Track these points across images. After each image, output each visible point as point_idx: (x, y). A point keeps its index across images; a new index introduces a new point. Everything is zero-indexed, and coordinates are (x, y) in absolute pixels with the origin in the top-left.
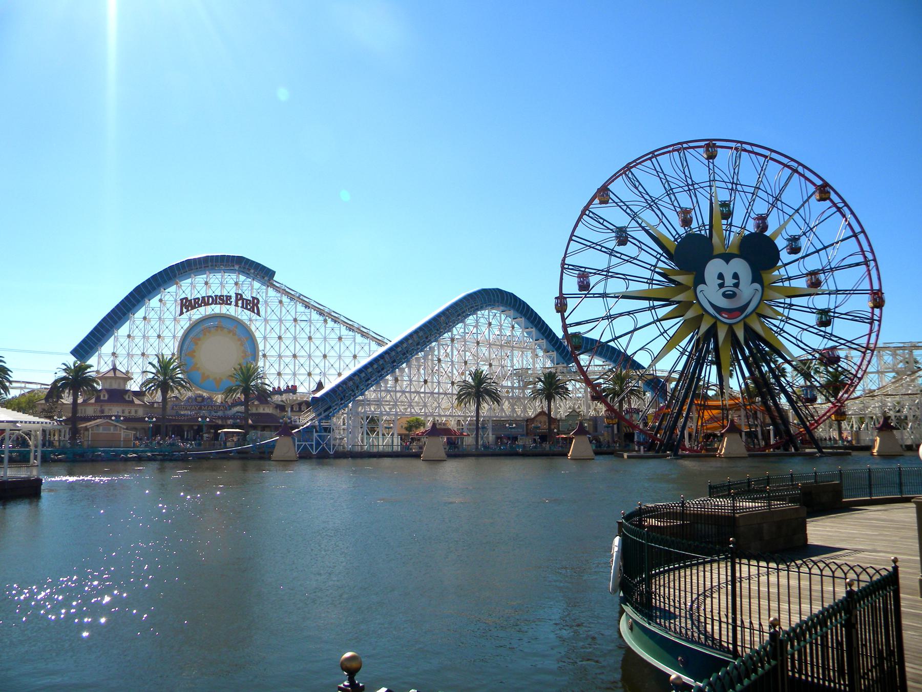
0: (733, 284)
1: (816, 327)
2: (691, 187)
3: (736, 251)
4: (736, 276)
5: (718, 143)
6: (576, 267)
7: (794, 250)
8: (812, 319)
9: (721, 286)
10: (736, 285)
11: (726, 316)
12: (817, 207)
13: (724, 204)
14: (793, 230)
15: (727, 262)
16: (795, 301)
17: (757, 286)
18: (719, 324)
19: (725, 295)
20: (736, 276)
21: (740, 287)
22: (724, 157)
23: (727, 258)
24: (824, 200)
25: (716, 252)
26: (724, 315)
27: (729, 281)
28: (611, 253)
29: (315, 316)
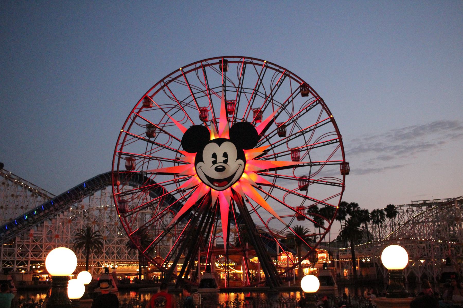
0: (223, 161)
1: (299, 192)
2: (209, 92)
3: (227, 137)
4: (225, 155)
5: (229, 59)
6: (126, 154)
7: (282, 133)
8: (294, 186)
9: (214, 162)
10: (225, 162)
11: (217, 185)
12: (300, 101)
13: (232, 103)
14: (283, 118)
15: (220, 146)
16: (280, 172)
17: (241, 161)
18: (213, 190)
19: (216, 169)
20: (225, 155)
21: (228, 163)
22: (232, 69)
23: (219, 142)
24: (307, 95)
25: (213, 138)
26: (216, 184)
27: (221, 159)
28: (149, 141)
29: (29, 194)
